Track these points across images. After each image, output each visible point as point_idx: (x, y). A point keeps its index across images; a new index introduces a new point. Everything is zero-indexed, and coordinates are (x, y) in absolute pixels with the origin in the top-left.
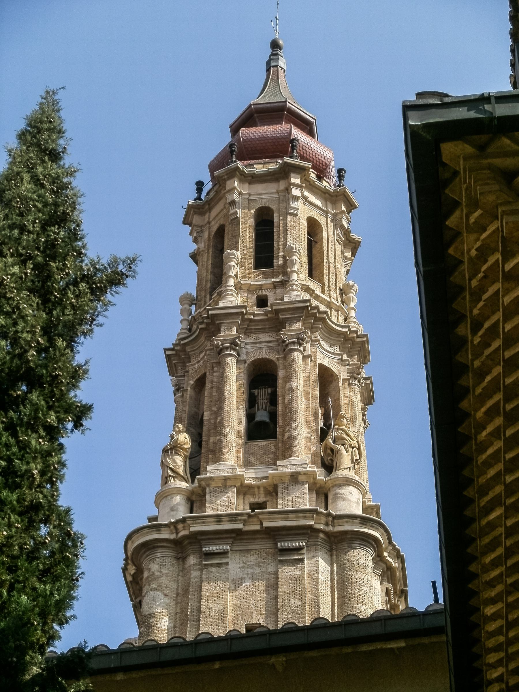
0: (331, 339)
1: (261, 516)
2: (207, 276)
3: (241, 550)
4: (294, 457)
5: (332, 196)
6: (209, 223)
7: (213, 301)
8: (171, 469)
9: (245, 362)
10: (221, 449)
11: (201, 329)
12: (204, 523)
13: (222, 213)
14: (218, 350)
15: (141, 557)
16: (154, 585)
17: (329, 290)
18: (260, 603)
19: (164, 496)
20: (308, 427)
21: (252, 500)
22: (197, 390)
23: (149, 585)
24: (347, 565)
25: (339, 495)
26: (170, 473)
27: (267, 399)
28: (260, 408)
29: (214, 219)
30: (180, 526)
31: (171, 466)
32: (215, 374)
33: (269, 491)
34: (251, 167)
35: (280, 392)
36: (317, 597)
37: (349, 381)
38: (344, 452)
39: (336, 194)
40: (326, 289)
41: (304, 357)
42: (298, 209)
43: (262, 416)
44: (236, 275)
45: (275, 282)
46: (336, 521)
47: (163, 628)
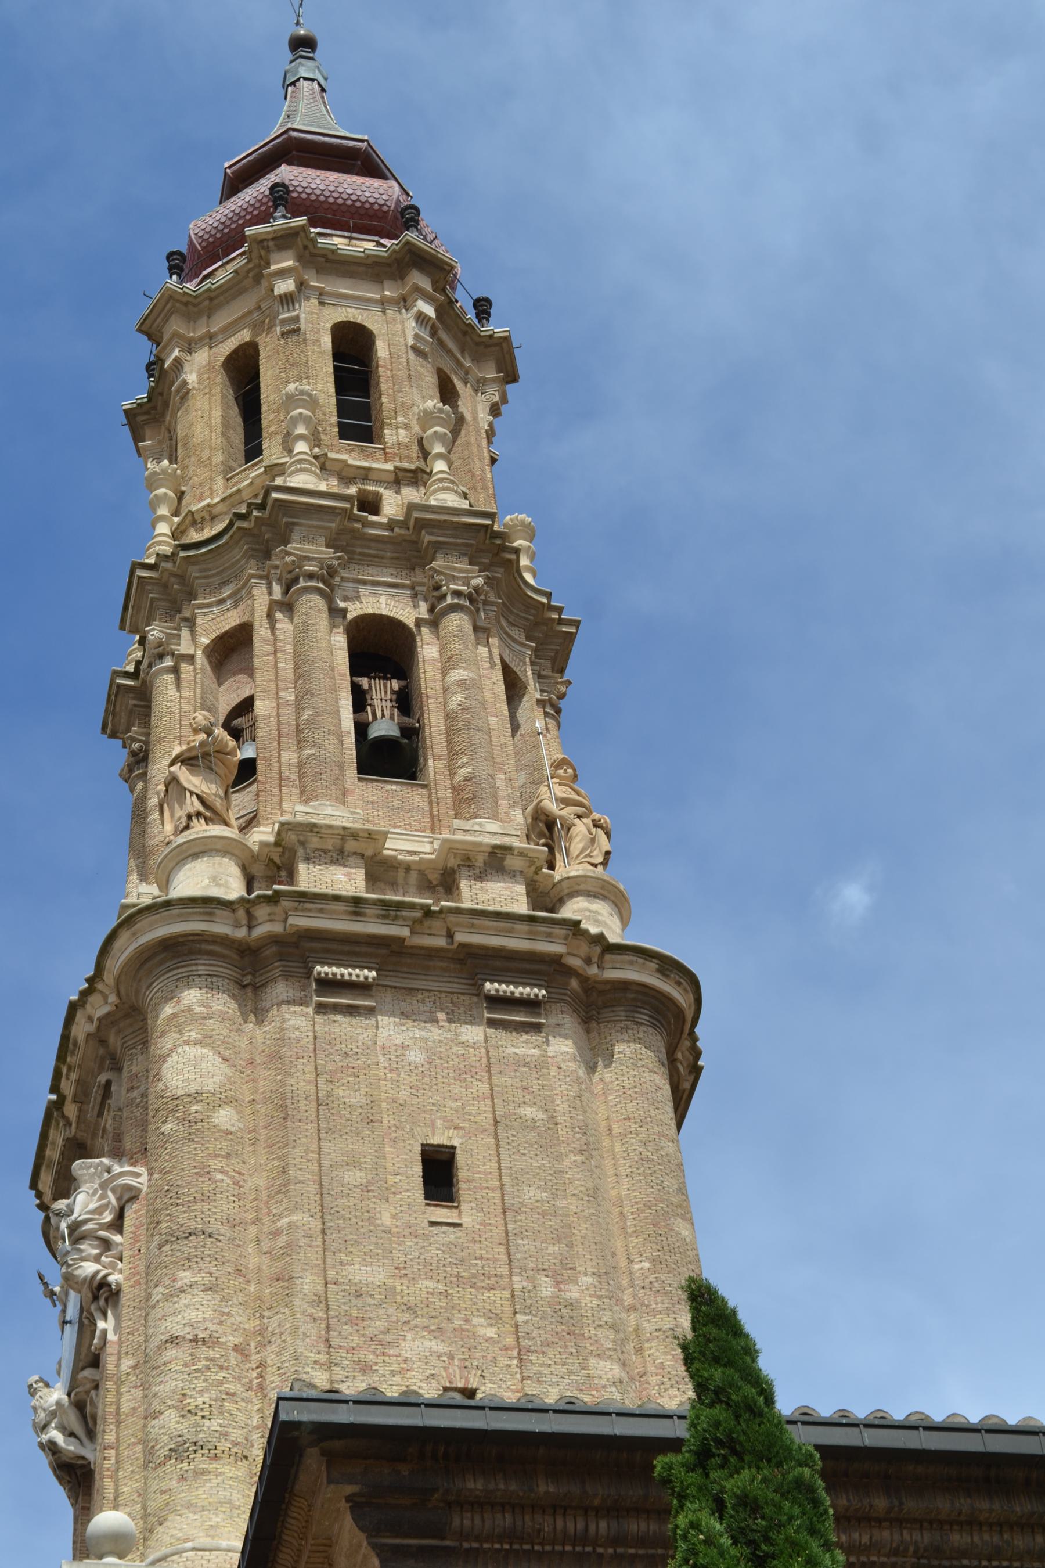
0: (511, 612)
3: (395, 987)
7: (251, 484)
11: (239, 528)
12: (321, 911)
19: (190, 852)
22: (214, 660)
23: (181, 1032)
27: (391, 700)
28: (379, 714)
30: (262, 912)
33: (431, 882)
46: (608, 957)
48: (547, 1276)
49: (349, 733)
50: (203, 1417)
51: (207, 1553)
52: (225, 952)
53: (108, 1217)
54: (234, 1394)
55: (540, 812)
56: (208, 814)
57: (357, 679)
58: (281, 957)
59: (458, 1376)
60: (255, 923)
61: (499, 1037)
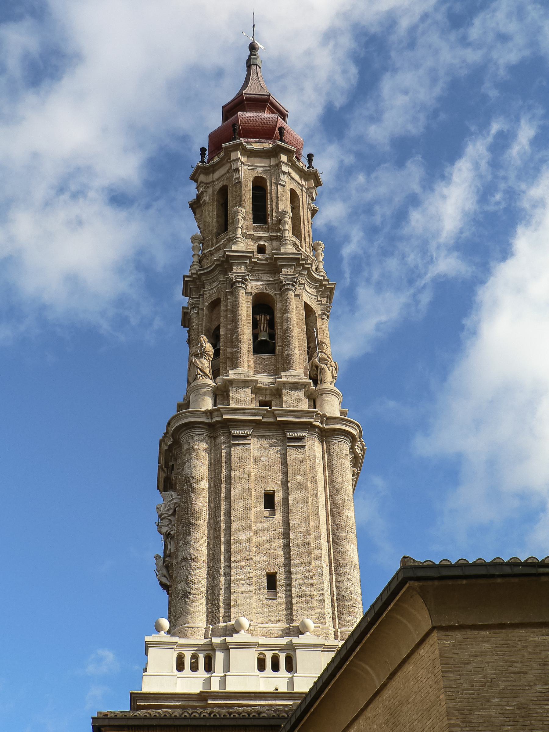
1: (275, 413)
3: (258, 435)
4: (293, 370)
8: (199, 368)
9: (250, 293)
10: (237, 359)
11: (216, 264)
15: (181, 433)
17: (306, 246)
18: (274, 475)
20: (300, 349)
21: (261, 398)
26: (199, 372)
28: (262, 330)
29: (218, 180)
31: (200, 367)
35: (278, 319)
36: (315, 474)
37: (322, 317)
40: (304, 245)
41: (295, 295)
42: (286, 182)
43: (263, 337)
44: (242, 226)
47: (202, 488)
48: (301, 534)
50: (193, 584)
51: (192, 628)
52: (204, 427)
53: (171, 512)
55: (313, 363)
56: (202, 374)
59: (271, 568)
61: (291, 451)
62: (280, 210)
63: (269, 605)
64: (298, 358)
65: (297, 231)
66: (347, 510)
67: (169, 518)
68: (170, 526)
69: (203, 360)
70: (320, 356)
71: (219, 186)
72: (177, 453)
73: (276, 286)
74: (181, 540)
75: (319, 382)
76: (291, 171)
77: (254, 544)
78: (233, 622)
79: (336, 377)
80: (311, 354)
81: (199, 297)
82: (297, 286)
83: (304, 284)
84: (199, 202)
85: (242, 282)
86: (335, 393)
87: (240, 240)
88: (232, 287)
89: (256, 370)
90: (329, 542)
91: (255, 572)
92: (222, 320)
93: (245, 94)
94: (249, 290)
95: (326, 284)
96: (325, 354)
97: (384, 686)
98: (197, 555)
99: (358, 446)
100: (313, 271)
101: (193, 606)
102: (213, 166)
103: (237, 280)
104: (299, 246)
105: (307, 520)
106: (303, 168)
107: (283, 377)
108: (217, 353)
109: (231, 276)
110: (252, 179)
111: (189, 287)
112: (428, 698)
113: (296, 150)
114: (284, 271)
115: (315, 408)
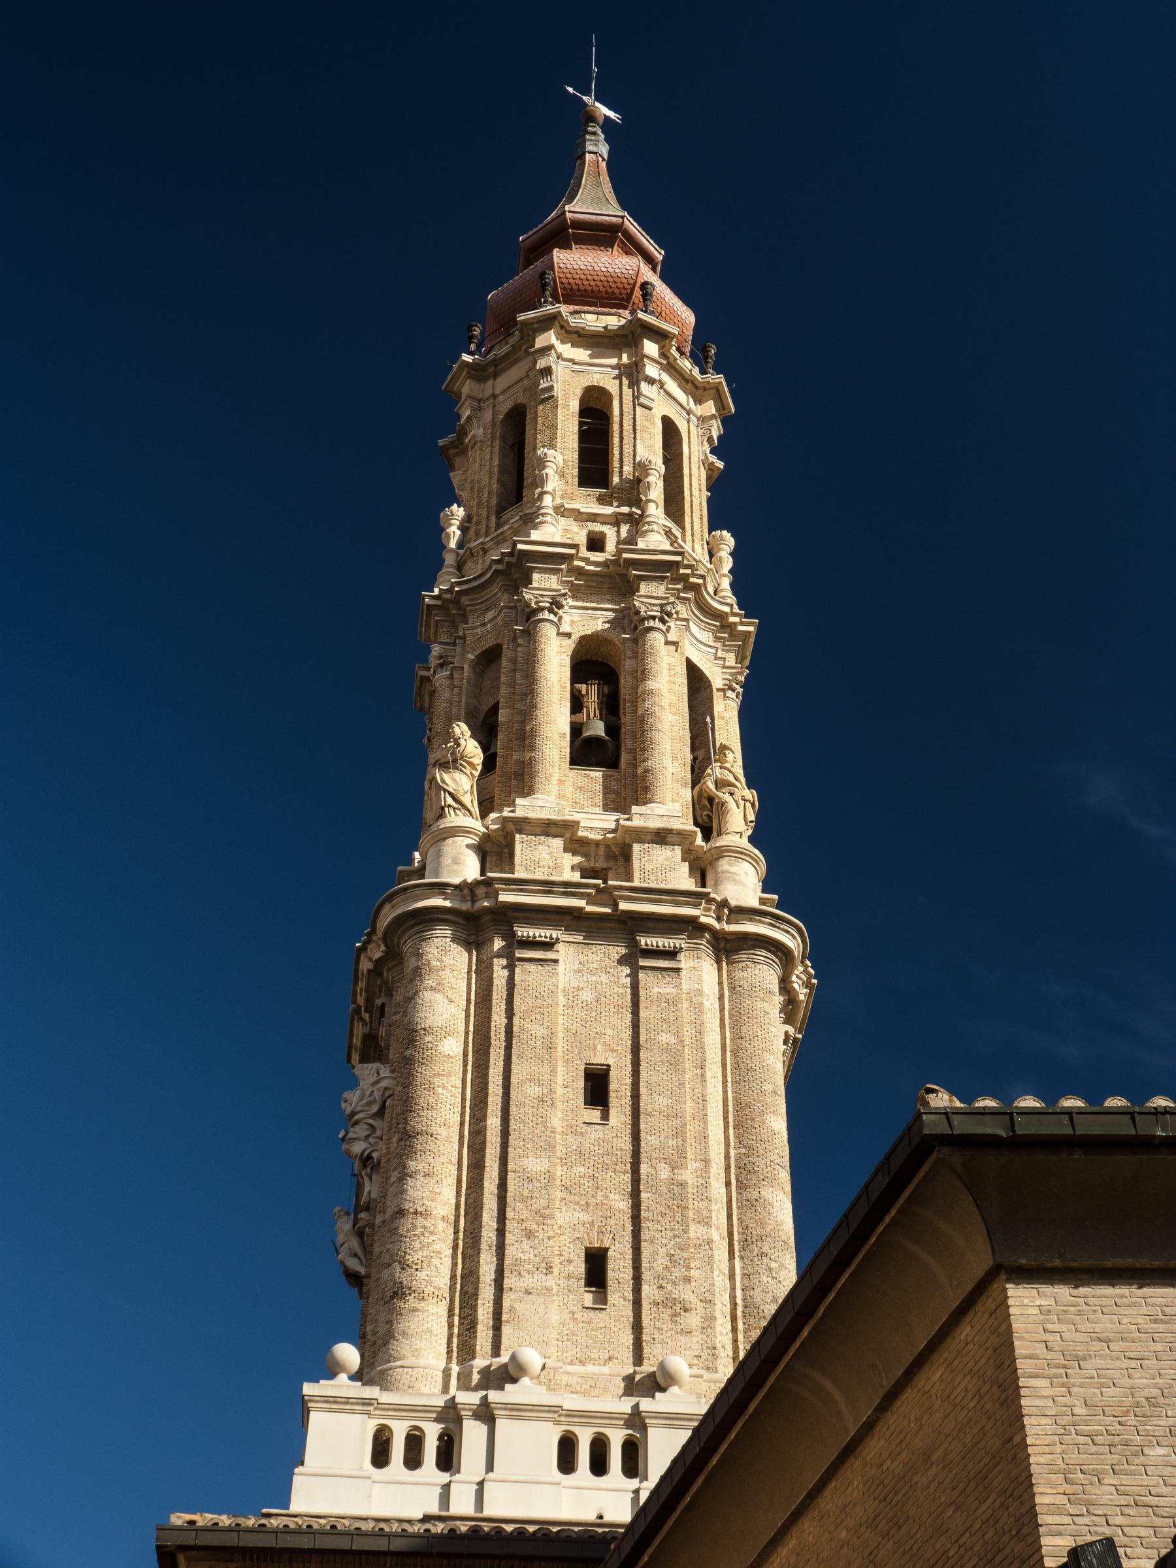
2: (490, 483)
4: (658, 802)
5: (697, 388)
6: (494, 396)
7: (511, 528)
8: (451, 794)
9: (568, 635)
10: (532, 775)
11: (496, 571)
13: (521, 383)
14: (528, 610)
16: (429, 982)
17: (693, 541)
18: (609, 1032)
19: (440, 837)
20: (674, 759)
24: (746, 987)
25: (728, 875)
26: (450, 801)
28: (592, 715)
29: (503, 392)
30: (481, 891)
31: (451, 790)
32: (519, 649)
34: (578, 316)
35: (625, 693)
37: (725, 694)
38: (732, 804)
39: (703, 385)
40: (689, 538)
41: (667, 643)
44: (554, 490)
45: (620, 514)
47: (446, 1053)
48: (666, 1163)
49: (565, 734)
50: (417, 1270)
51: (411, 1370)
53: (375, 1108)
54: (439, 1252)
56: (456, 805)
57: (577, 686)
58: (495, 922)
59: (596, 1239)
60: (476, 899)
62: (638, 459)
63: (590, 1322)
64: (669, 776)
65: (674, 505)
66: (771, 1115)
67: (371, 1121)
68: (372, 1140)
69: (457, 775)
70: (719, 776)
71: (505, 406)
72: (392, 978)
73: (626, 621)
74: (394, 1170)
75: (715, 833)
76: (665, 377)
77: (558, 1182)
78: (504, 1358)
79: (751, 822)
80: (698, 771)
81: (455, 641)
82: (672, 624)
83: (687, 620)
84: (462, 443)
85: (551, 611)
86: (752, 858)
87: (548, 519)
88: (528, 619)
89: (576, 803)
90: (728, 1184)
91: (559, 1247)
92: (503, 691)
93: (569, 212)
94: (565, 628)
95: (735, 624)
96: (730, 772)
97: (867, 1428)
98: (428, 1203)
99: (798, 977)
100: (708, 594)
101: (416, 1319)
102: (496, 362)
103: (540, 604)
104: (676, 538)
105: (680, 1133)
106: (693, 372)
107: (635, 817)
108: (489, 763)
109: (527, 597)
110: (579, 392)
111: (432, 620)
112: (981, 1445)
113: (677, 333)
114: (645, 588)
115: (704, 885)
